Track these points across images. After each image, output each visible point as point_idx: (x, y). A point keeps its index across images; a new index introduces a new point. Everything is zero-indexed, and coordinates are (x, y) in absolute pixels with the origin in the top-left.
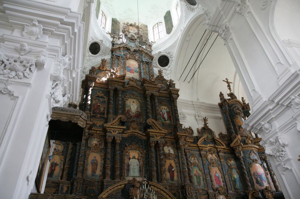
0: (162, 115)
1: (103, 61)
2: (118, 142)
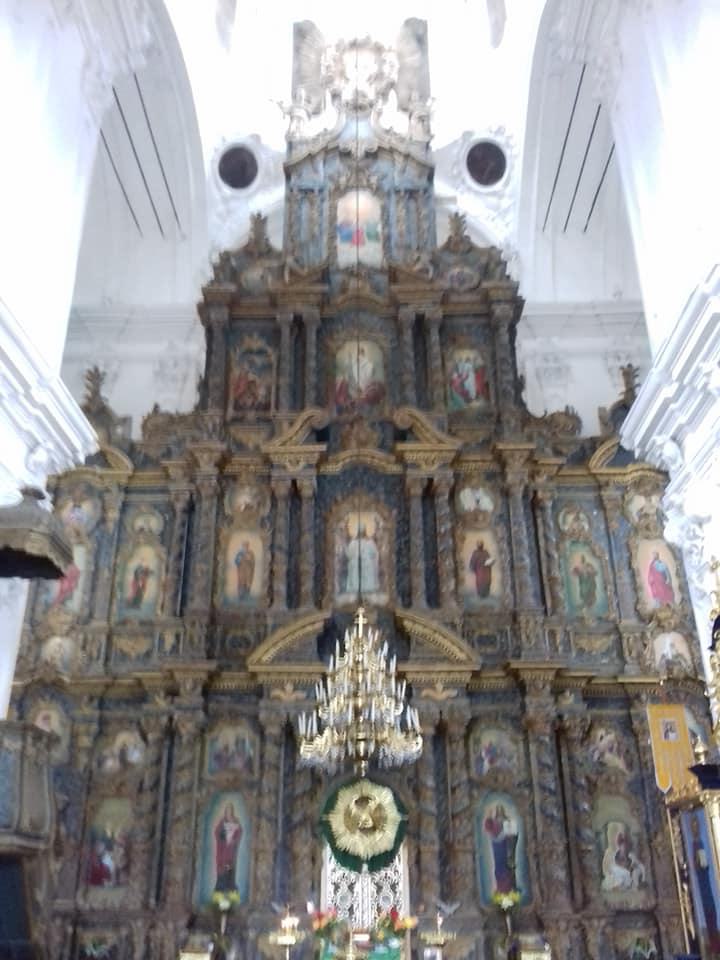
0: (458, 381)
1: (259, 222)
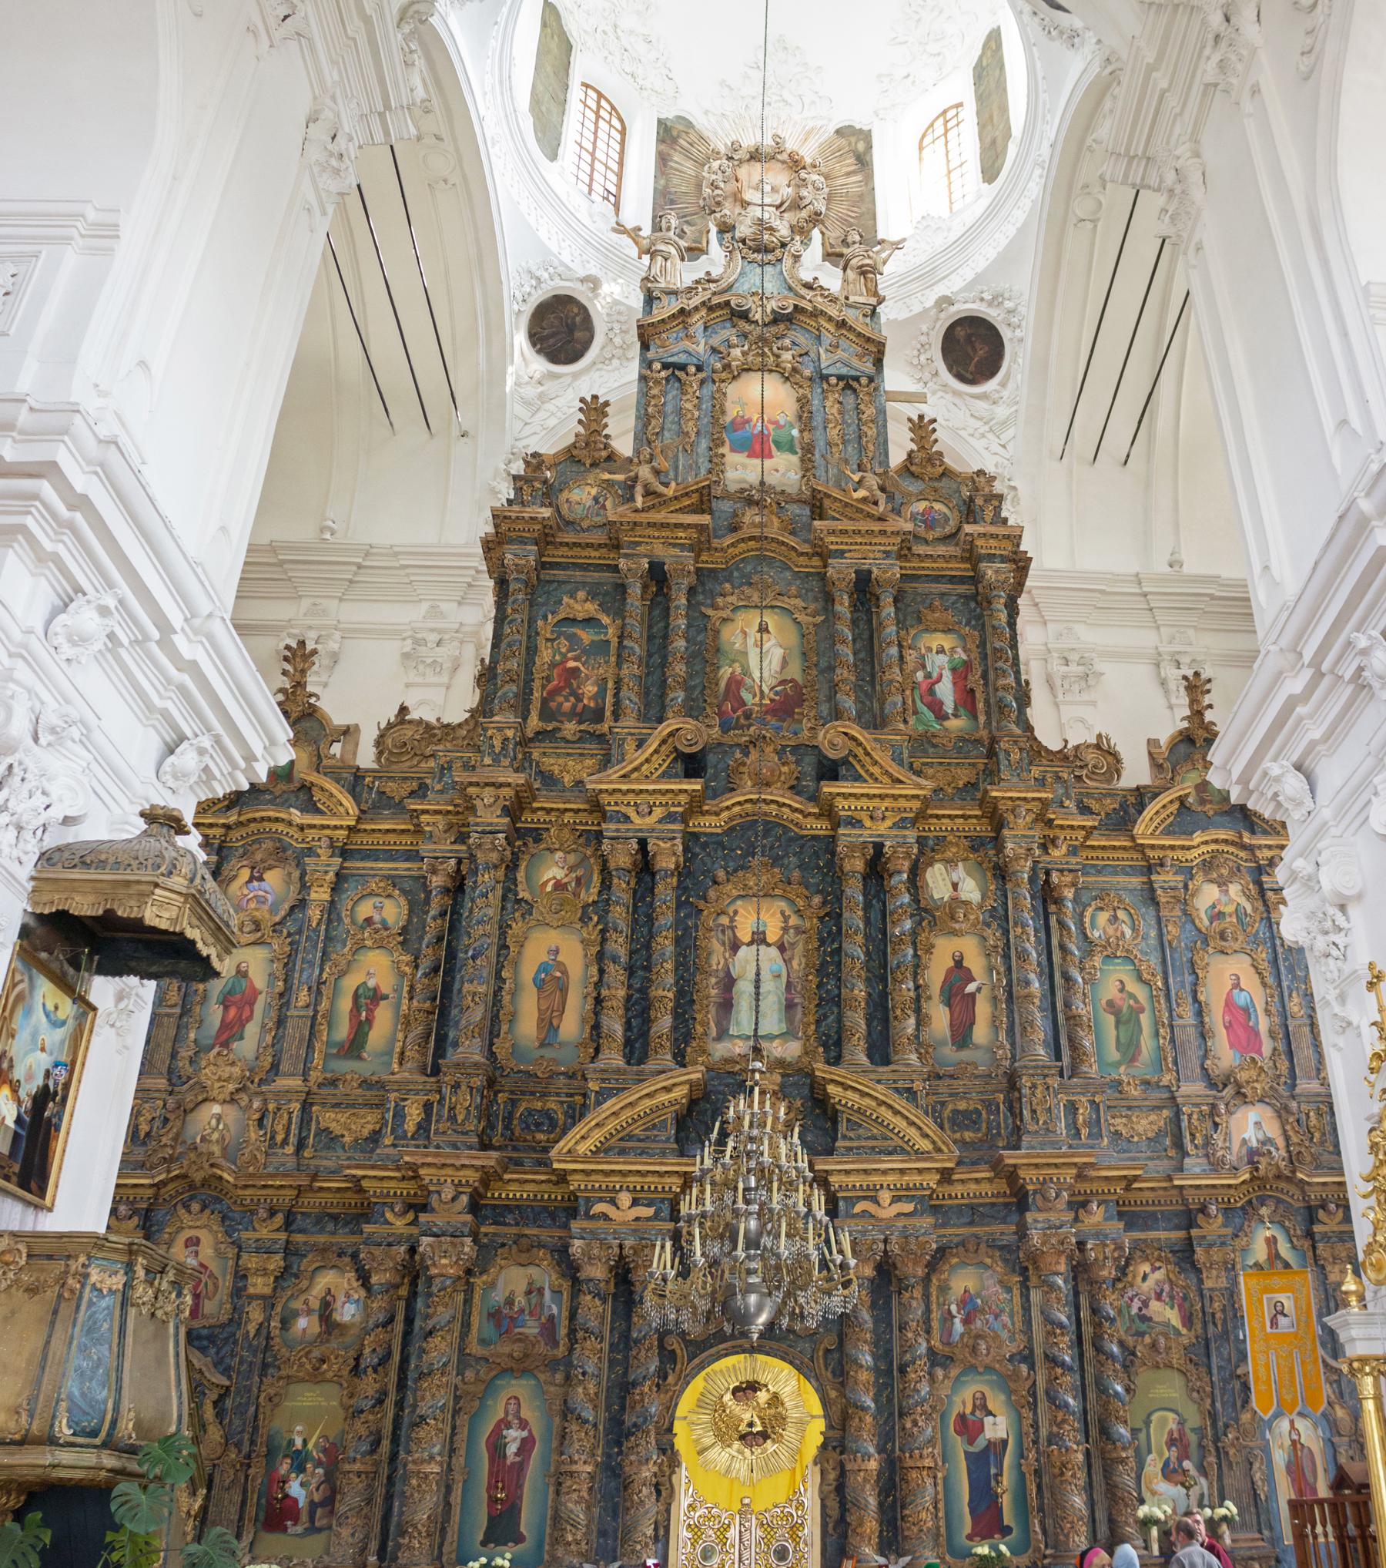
0: (924, 687)
1: (595, 410)
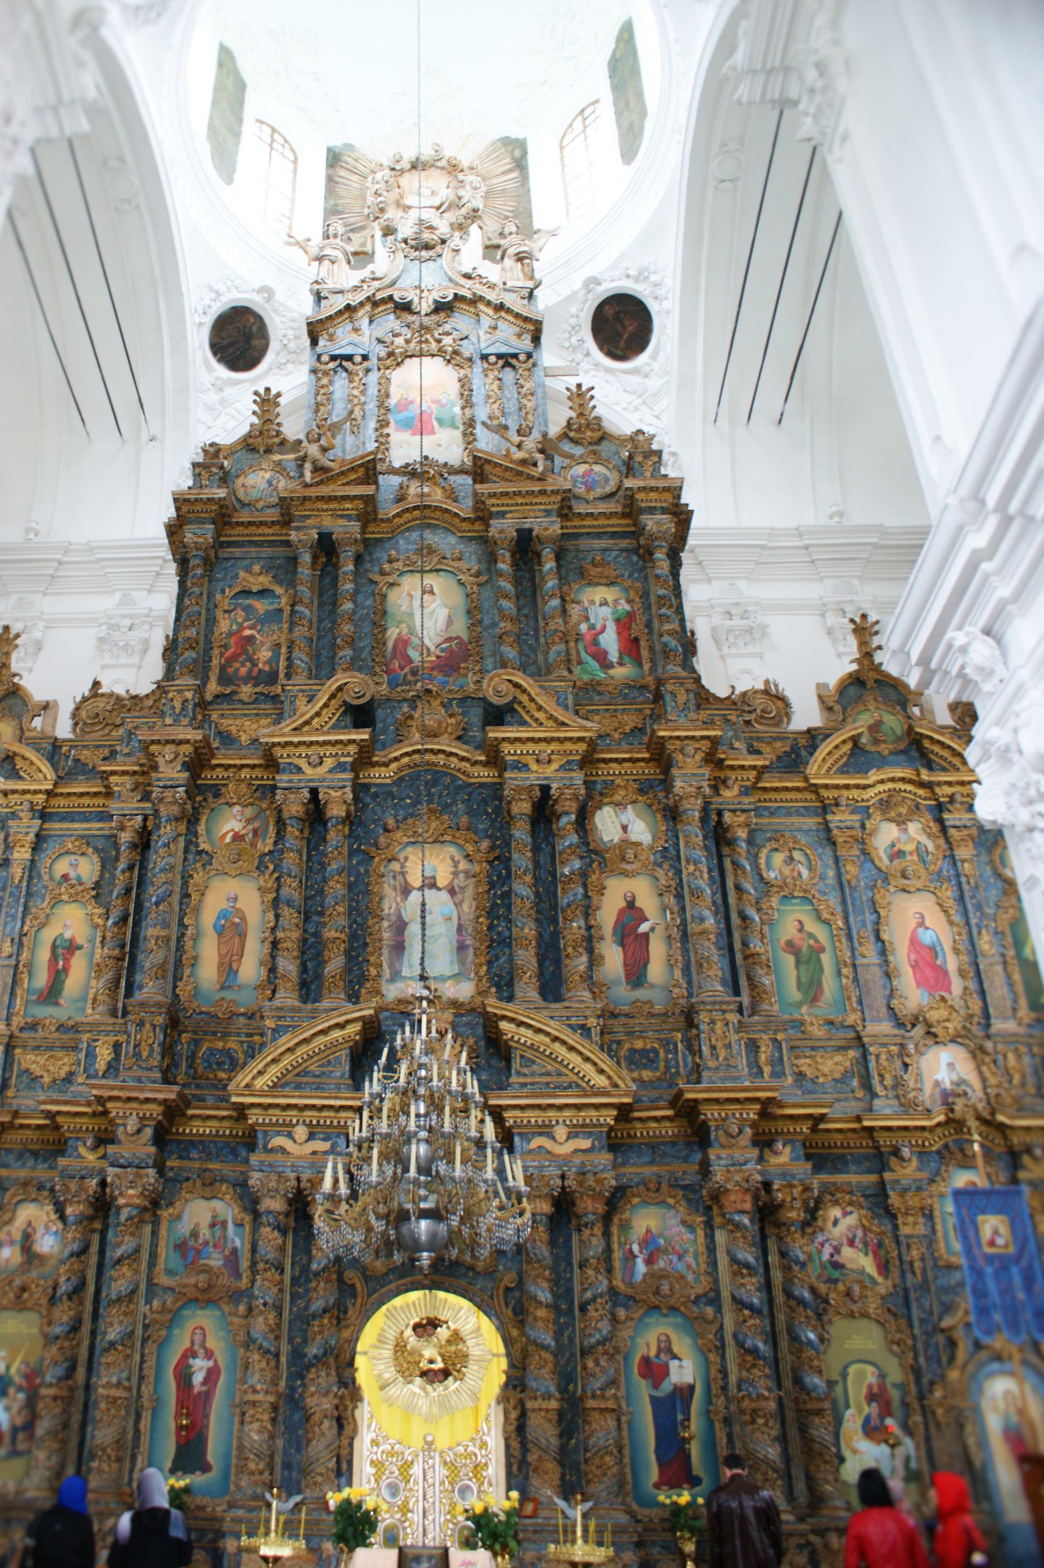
2: (335, 812)
